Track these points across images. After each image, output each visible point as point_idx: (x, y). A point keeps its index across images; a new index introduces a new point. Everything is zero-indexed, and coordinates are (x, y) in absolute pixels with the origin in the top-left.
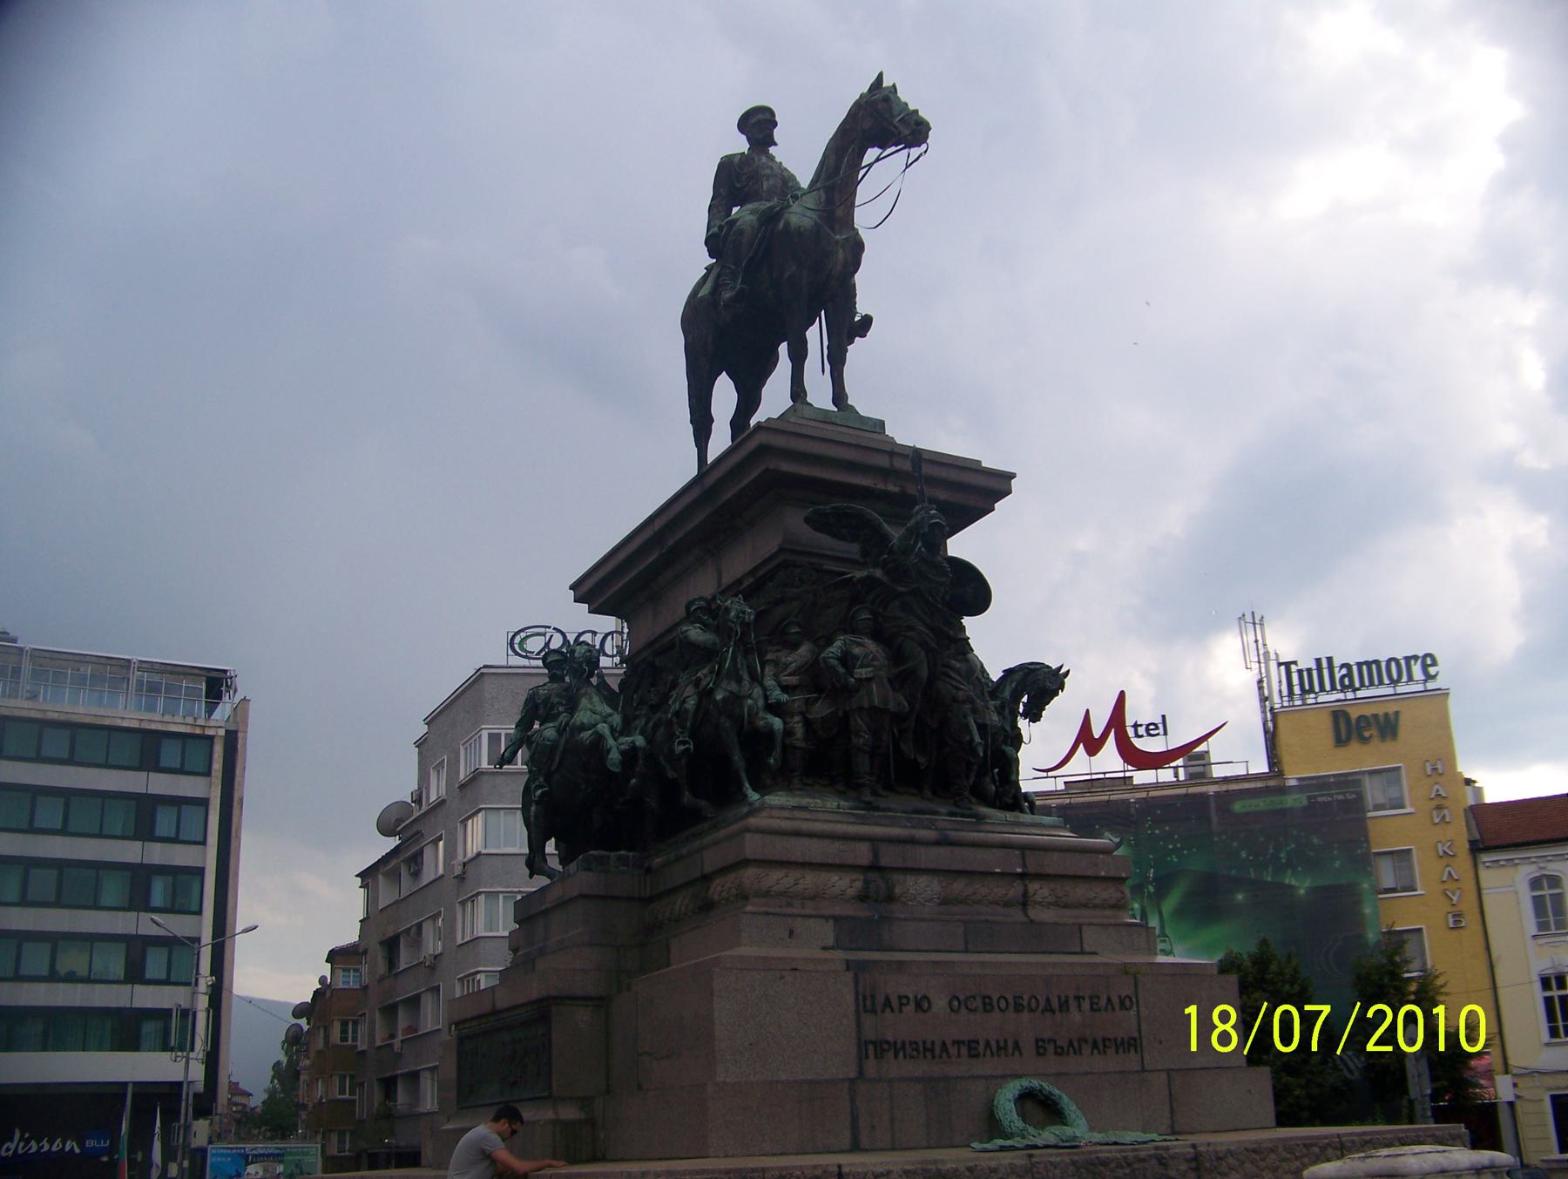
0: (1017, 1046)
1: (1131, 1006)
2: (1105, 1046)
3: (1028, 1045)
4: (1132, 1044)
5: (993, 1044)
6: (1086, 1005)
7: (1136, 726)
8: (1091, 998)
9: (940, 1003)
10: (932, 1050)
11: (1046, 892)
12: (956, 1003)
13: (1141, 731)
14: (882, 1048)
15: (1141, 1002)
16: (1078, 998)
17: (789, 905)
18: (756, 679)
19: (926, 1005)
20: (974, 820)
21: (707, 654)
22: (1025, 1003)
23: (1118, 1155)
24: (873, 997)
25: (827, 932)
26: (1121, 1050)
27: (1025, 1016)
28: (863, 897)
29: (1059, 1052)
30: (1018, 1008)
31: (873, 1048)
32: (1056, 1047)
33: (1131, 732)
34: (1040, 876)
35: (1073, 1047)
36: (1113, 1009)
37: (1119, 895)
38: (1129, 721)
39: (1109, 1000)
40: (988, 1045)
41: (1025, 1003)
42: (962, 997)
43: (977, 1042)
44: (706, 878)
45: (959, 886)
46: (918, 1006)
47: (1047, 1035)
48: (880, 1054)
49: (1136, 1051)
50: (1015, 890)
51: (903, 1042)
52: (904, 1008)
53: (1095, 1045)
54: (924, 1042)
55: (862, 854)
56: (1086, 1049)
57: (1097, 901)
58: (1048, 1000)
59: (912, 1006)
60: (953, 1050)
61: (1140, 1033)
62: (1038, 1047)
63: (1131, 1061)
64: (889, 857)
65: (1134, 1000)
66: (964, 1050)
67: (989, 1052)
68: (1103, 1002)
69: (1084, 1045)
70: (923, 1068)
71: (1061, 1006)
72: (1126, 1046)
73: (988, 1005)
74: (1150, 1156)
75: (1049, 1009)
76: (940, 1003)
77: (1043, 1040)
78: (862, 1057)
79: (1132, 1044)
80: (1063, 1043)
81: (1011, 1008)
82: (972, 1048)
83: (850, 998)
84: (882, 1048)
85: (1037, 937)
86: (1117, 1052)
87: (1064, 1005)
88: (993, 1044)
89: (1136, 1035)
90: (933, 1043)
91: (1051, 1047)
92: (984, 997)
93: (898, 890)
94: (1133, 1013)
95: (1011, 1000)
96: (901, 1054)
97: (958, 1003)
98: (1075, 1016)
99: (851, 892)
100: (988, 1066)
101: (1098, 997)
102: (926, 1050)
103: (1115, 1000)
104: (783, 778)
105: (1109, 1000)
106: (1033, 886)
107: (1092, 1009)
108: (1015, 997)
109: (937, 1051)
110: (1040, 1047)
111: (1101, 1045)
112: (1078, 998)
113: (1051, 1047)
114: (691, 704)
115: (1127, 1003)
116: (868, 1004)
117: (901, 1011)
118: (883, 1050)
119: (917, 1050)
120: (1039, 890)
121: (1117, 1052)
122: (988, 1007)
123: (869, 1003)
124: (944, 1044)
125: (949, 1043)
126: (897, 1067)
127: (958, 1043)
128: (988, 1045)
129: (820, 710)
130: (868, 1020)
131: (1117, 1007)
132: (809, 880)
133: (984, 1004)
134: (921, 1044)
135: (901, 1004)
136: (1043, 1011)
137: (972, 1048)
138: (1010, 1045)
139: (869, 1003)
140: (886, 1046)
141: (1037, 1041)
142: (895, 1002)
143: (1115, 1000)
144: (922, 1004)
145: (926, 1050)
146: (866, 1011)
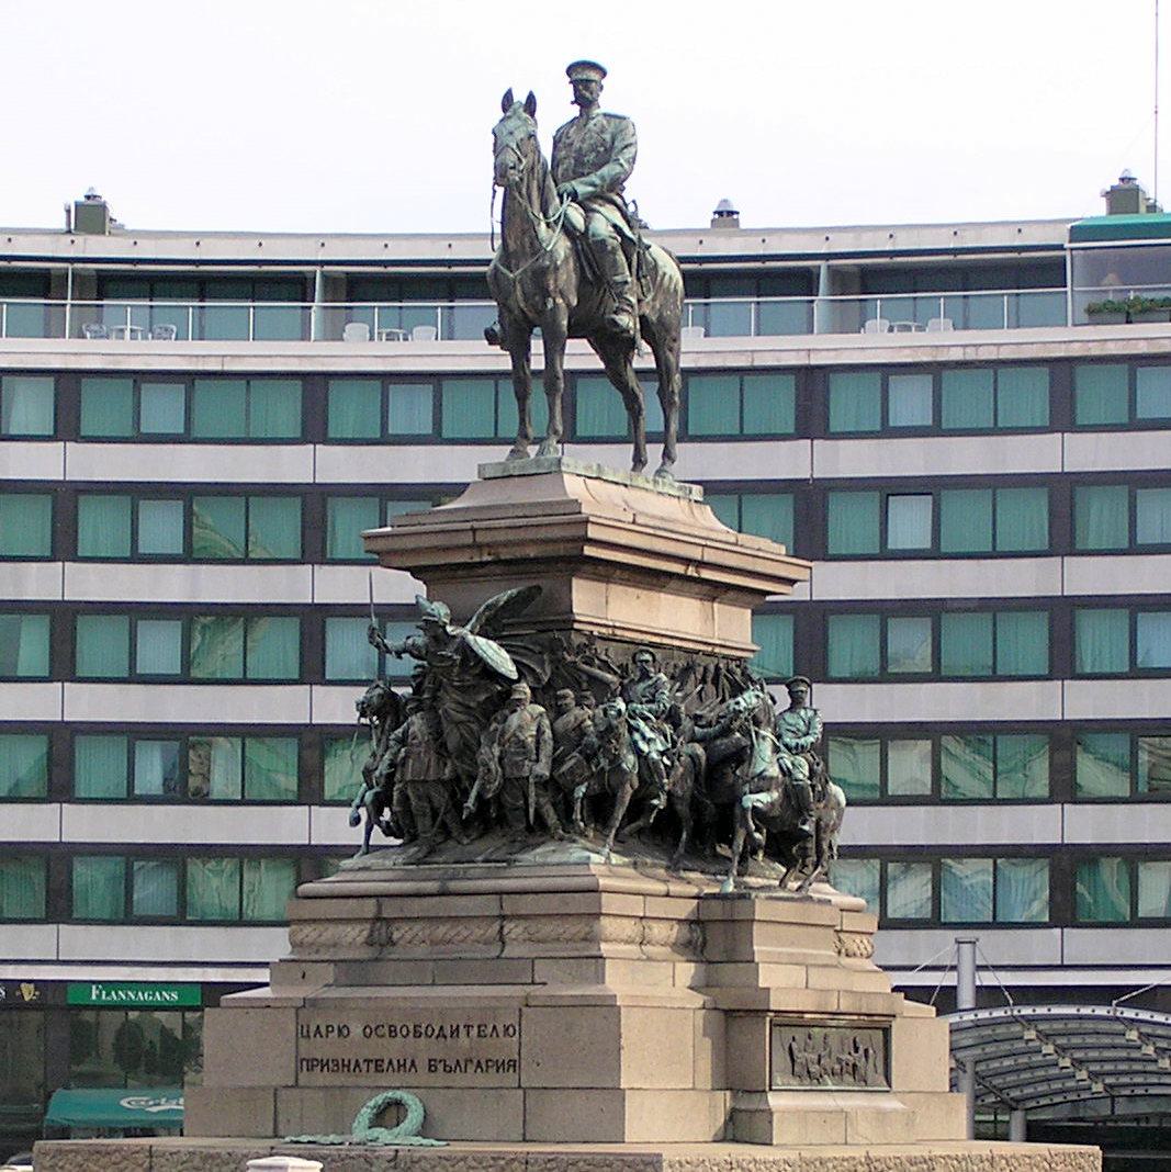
1: (514, 1034)
2: (488, 1067)
3: (422, 1064)
4: (513, 1065)
5: (395, 1063)
6: (474, 1032)
8: (479, 1027)
9: (357, 1030)
10: (349, 1066)
11: (519, 930)
12: (368, 1030)
14: (312, 1064)
15: (523, 1028)
16: (468, 1027)
17: (317, 952)
19: (346, 1032)
20: (505, 864)
22: (423, 1031)
23: (335, 1153)
24: (308, 1026)
26: (501, 1070)
28: (369, 943)
29: (448, 1070)
30: (417, 1035)
32: (445, 1066)
36: (498, 1036)
37: (587, 929)
39: (494, 1027)
40: (390, 1063)
41: (423, 1031)
42: (373, 1027)
43: (383, 1061)
45: (442, 930)
49: (515, 1071)
51: (328, 1061)
52: (330, 1035)
53: (479, 1065)
54: (343, 1060)
55: (369, 908)
56: (471, 1068)
57: (566, 936)
58: (441, 1028)
60: (364, 1066)
61: (519, 1054)
62: (430, 1066)
63: (510, 1078)
65: (517, 1028)
66: (372, 1066)
67: (391, 1069)
69: (469, 1066)
71: (452, 1033)
72: (506, 1066)
73: (393, 1032)
74: (360, 1156)
76: (357, 1030)
77: (435, 1060)
79: (513, 1065)
81: (411, 1035)
83: (292, 1027)
84: (312, 1064)
85: (498, 969)
86: (498, 1071)
87: (455, 1032)
88: (395, 1063)
89: (516, 1057)
90: (349, 1061)
91: (441, 1067)
92: (391, 1026)
93: (396, 936)
94: (515, 1039)
95: (411, 1028)
96: (326, 1068)
97: (369, 1032)
98: (463, 1039)
99: (360, 939)
101: (486, 1026)
102: (341, 1066)
103: (500, 1029)
105: (494, 1027)
106: (508, 926)
107: (479, 1035)
108: (415, 1027)
109: (352, 1067)
112: (468, 1027)
113: (441, 1067)
115: (511, 1030)
116: (303, 1033)
117: (327, 1036)
118: (313, 1066)
119: (337, 1065)
120: (513, 929)
121: (498, 1071)
122: (393, 1034)
123: (305, 1031)
124: (357, 1061)
125: (361, 1061)
126: (321, 1078)
128: (390, 1063)
130: (303, 1041)
131: (501, 1035)
132: (331, 932)
133: (390, 1032)
134: (340, 1063)
135: (328, 1031)
136: (437, 1037)
138: (408, 1065)
139: (305, 1031)
140: (315, 1063)
141: (430, 1061)
142: (323, 1030)
143: (500, 1029)
144: (343, 1031)
145: (341, 1066)
146: (303, 1036)
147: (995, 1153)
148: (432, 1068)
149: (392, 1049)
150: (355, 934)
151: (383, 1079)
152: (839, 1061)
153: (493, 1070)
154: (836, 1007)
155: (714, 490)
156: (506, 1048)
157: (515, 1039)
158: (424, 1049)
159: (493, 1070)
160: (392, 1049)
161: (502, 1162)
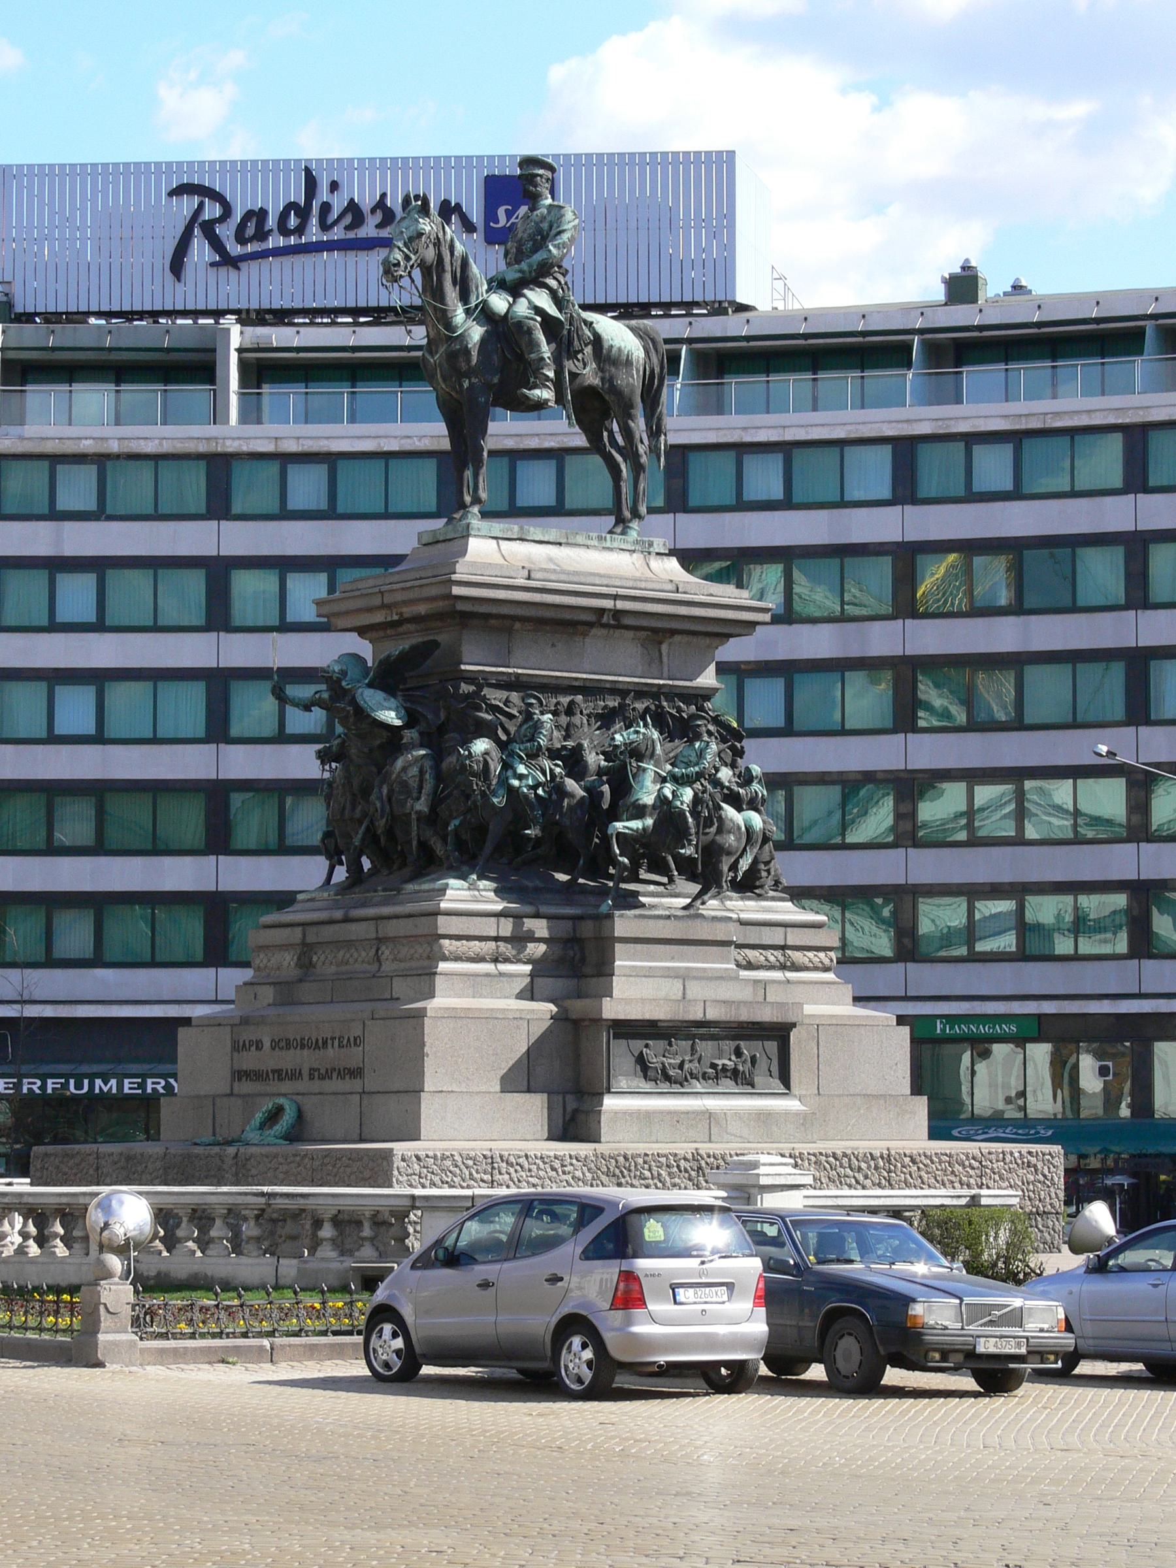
0: (300, 1073)
3: (305, 1073)
6: (336, 1042)
9: (267, 1044)
27: (306, 1052)
30: (303, 1047)
31: (240, 1075)
46: (257, 1048)
47: (315, 1066)
48: (239, 1080)
58: (317, 1041)
59: (253, 1048)
62: (310, 1075)
63: (356, 1085)
68: (345, 1042)
71: (323, 1043)
73: (289, 1045)
75: (317, 1047)
76: (267, 1044)
78: (233, 1080)
79: (356, 1073)
80: (323, 1071)
94: (361, 1048)
97: (275, 1045)
103: (352, 1039)
112: (333, 1039)
113: (316, 1074)
116: (238, 1047)
127: (274, 1071)
141: (310, 1070)
143: (352, 1039)
144: (259, 1045)
147: (893, 1152)
148: (311, 1077)
149: (289, 1059)
152: (713, 1066)
153: (347, 1077)
154: (702, 1015)
155: (690, 558)
156: (353, 1056)
157: (361, 1048)
158: (305, 1059)
159: (347, 1077)
161: (298, 1158)
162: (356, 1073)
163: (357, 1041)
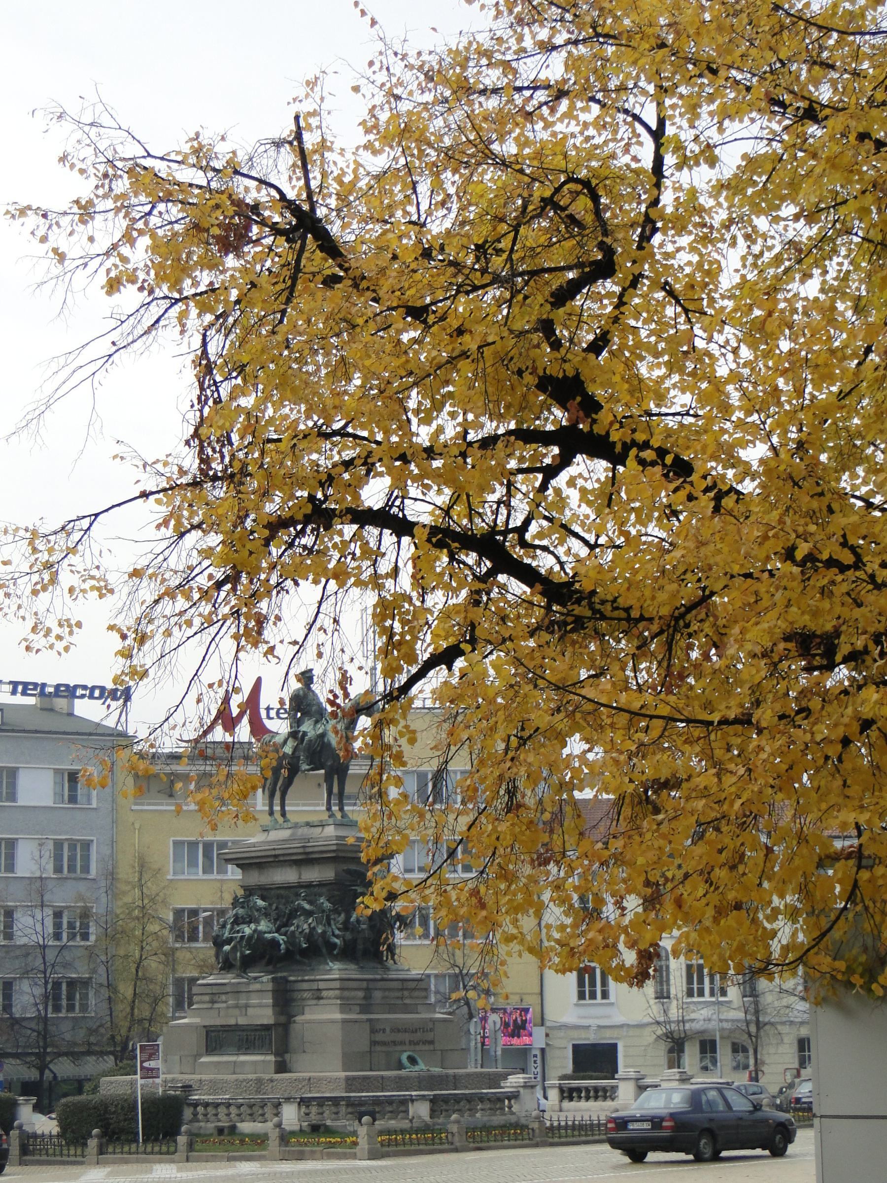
7: (268, 709)
9: (388, 1030)
13: (273, 714)
18: (329, 924)
21: (309, 914)
25: (357, 1008)
31: (374, 1043)
33: (263, 713)
34: (406, 989)
35: (417, 1043)
38: (263, 704)
44: (318, 990)
45: (387, 993)
50: (399, 994)
55: (364, 984)
63: (431, 1047)
64: (371, 985)
70: (384, 1048)
73: (399, 1031)
76: (388, 1030)
79: (432, 1042)
82: (394, 1043)
85: (406, 1009)
97: (392, 1031)
100: (399, 1048)
102: (384, 1043)
104: (335, 958)
110: (410, 1042)
111: (425, 1042)
114: (307, 931)
116: (373, 1031)
120: (406, 993)
129: (348, 936)
132: (353, 994)
137: (394, 1043)
144: (384, 1031)
149: (399, 1037)
150: (361, 994)
151: (404, 1048)
156: (429, 1036)
158: (407, 1037)
160: (399, 1037)
162: (432, 1042)
163: (431, 1030)
